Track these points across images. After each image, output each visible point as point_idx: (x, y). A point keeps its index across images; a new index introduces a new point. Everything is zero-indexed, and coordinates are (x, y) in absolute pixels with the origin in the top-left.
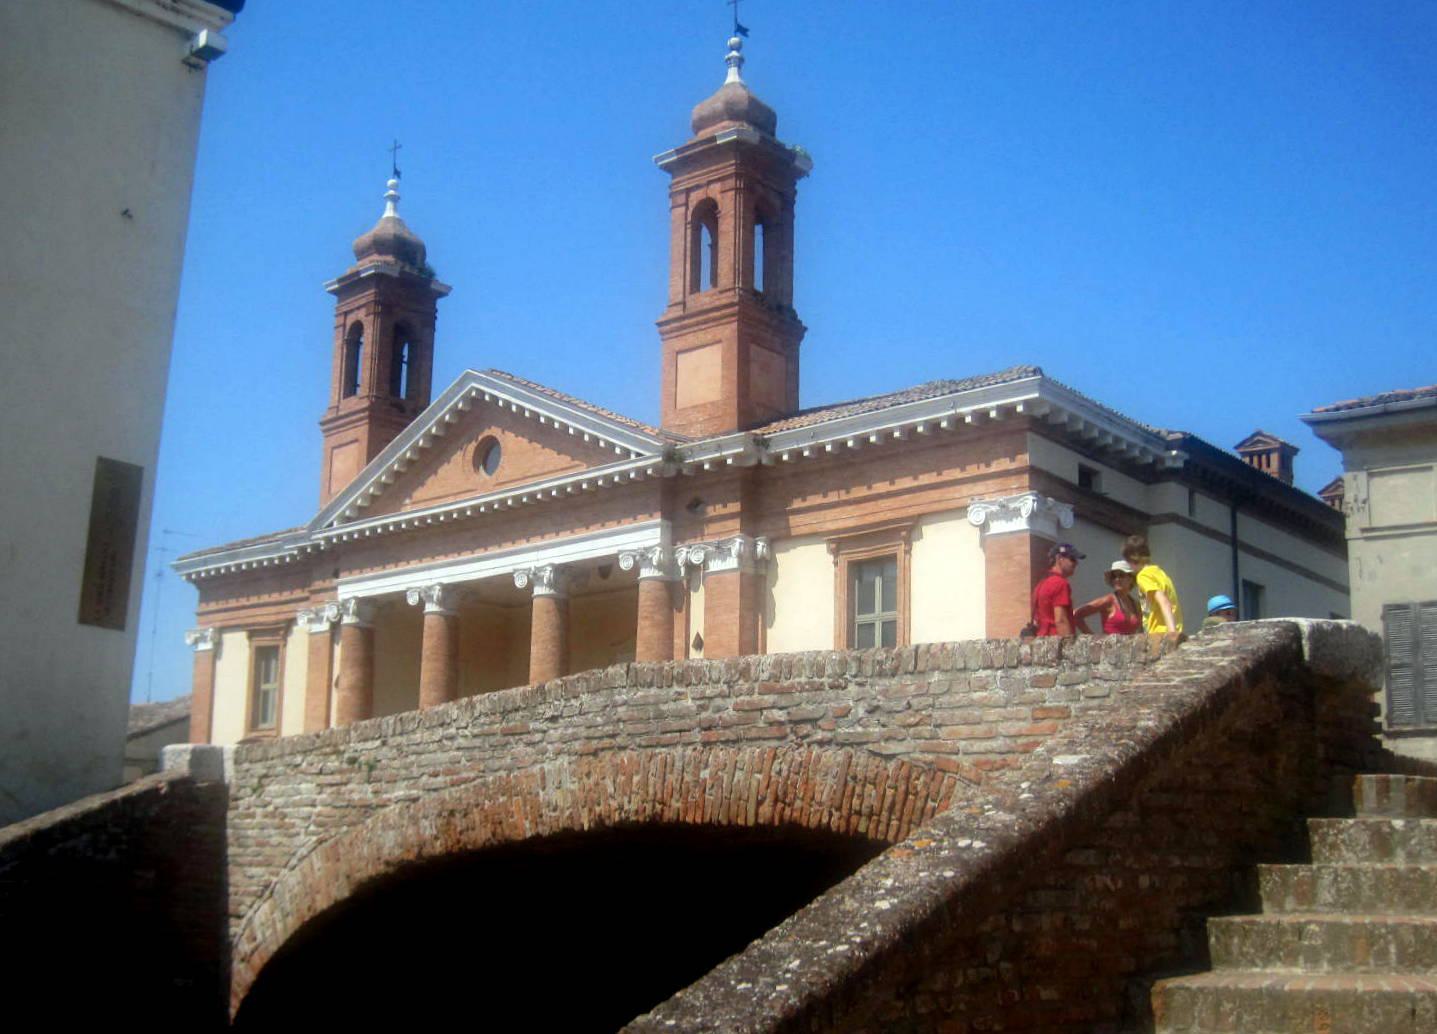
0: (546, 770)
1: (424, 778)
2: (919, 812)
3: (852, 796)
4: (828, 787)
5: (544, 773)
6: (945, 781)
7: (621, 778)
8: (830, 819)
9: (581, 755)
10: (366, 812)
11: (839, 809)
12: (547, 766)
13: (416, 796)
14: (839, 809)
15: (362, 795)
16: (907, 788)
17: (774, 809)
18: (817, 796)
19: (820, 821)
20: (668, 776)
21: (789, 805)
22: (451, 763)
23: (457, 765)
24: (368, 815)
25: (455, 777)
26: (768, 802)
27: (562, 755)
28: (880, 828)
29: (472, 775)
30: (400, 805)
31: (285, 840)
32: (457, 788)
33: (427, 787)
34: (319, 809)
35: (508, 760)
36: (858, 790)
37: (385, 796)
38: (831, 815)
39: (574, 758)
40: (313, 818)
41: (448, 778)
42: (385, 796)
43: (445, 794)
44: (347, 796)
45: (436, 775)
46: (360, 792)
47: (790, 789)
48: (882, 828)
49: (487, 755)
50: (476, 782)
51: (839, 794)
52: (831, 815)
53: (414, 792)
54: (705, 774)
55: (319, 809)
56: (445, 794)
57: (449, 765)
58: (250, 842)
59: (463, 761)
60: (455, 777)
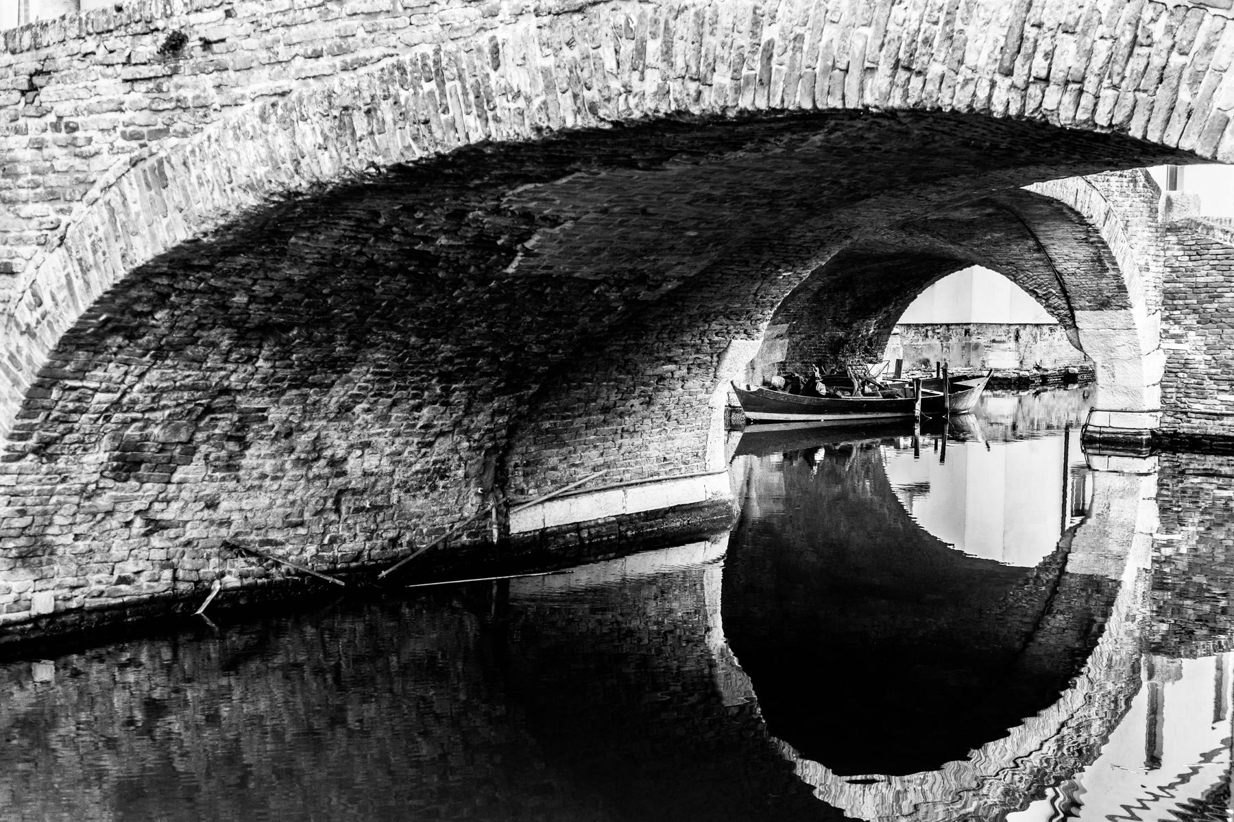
0: (500, 42)
1: (299, 61)
2: (1155, 75)
3: (1031, 57)
4: (990, 42)
5: (496, 46)
6: (1206, 24)
7: (628, 47)
8: (990, 97)
9: (558, 14)
10: (205, 116)
11: (1009, 73)
12: (501, 34)
13: (286, 89)
14: (1009, 73)
15: (197, 92)
16: (1136, 37)
17: (892, 84)
18: (970, 60)
19: (974, 95)
20: (707, 38)
21: (919, 73)
22: (341, 37)
23: (350, 40)
24: (208, 120)
25: (349, 58)
26: (884, 69)
27: (526, 16)
28: (1083, 102)
29: (377, 52)
30: (259, 103)
31: (77, 162)
32: (352, 74)
33: (303, 75)
34: (127, 116)
35: (436, 28)
36: (1045, 46)
37: (237, 91)
38: (993, 84)
39: (546, 20)
40: (121, 128)
41: (338, 61)
42: (237, 91)
43: (334, 83)
44: (173, 94)
45: (317, 55)
46: (196, 87)
47: (921, 49)
48: (1086, 101)
49: (402, 21)
50: (382, 64)
51: (1010, 51)
52: (993, 84)
53: (284, 84)
54: (769, 33)
55: (127, 116)
56: (334, 83)
57: (338, 40)
58: (20, 169)
59: (361, 33)
60: (349, 58)
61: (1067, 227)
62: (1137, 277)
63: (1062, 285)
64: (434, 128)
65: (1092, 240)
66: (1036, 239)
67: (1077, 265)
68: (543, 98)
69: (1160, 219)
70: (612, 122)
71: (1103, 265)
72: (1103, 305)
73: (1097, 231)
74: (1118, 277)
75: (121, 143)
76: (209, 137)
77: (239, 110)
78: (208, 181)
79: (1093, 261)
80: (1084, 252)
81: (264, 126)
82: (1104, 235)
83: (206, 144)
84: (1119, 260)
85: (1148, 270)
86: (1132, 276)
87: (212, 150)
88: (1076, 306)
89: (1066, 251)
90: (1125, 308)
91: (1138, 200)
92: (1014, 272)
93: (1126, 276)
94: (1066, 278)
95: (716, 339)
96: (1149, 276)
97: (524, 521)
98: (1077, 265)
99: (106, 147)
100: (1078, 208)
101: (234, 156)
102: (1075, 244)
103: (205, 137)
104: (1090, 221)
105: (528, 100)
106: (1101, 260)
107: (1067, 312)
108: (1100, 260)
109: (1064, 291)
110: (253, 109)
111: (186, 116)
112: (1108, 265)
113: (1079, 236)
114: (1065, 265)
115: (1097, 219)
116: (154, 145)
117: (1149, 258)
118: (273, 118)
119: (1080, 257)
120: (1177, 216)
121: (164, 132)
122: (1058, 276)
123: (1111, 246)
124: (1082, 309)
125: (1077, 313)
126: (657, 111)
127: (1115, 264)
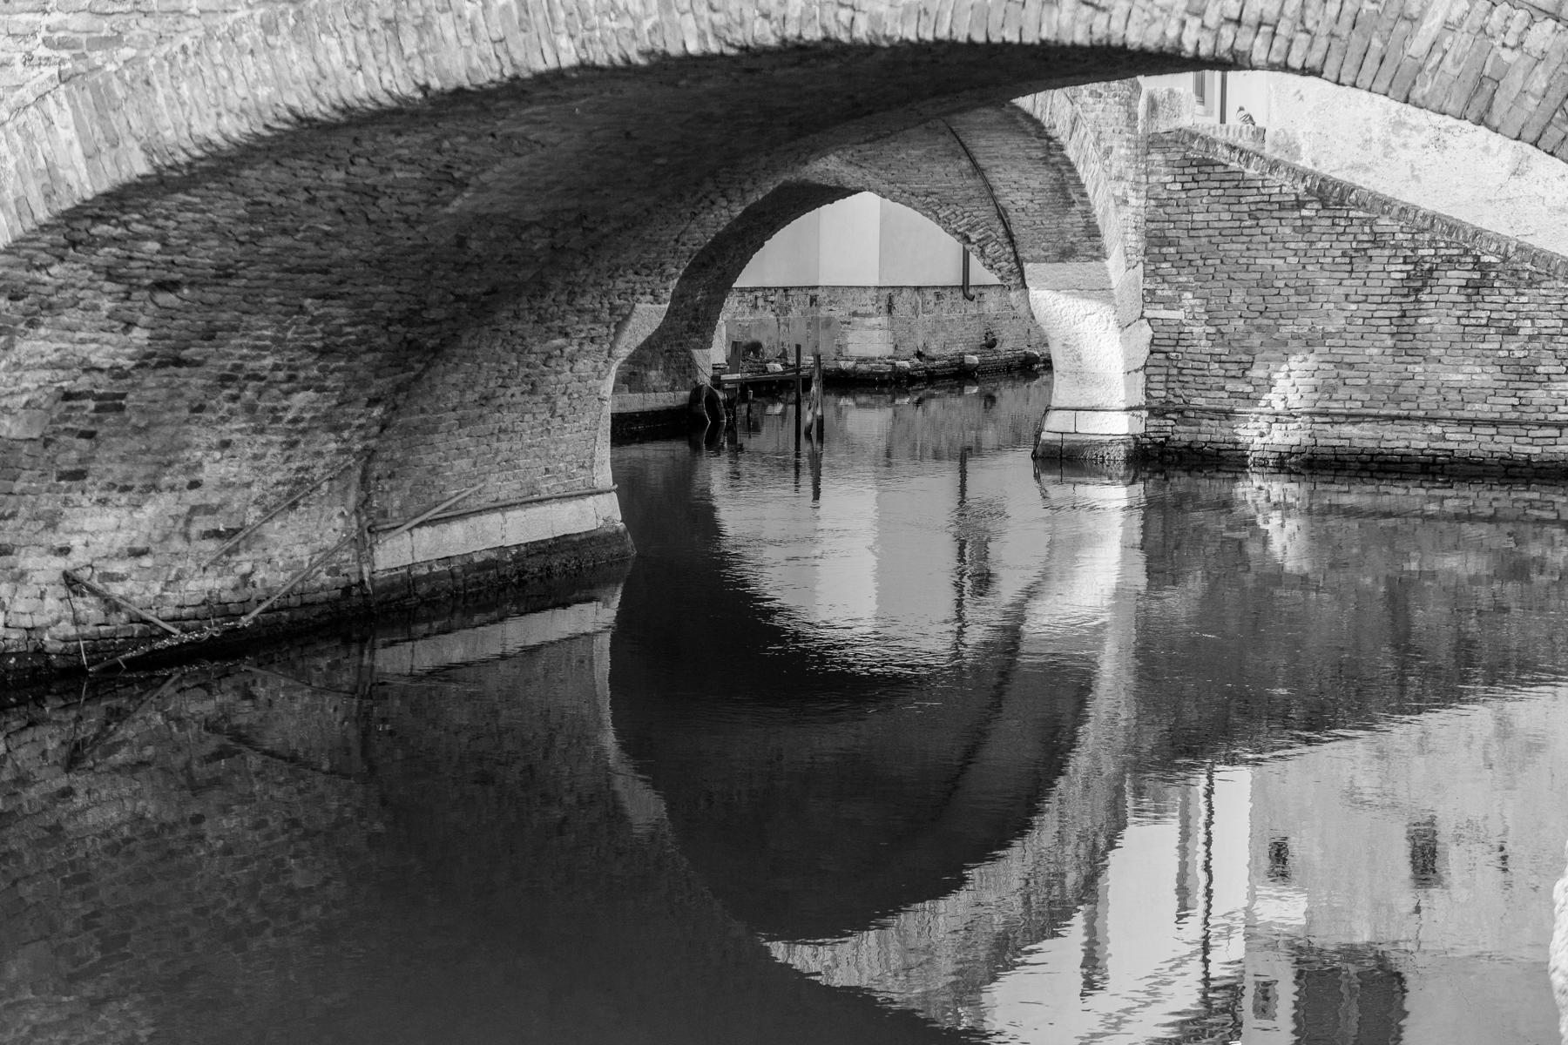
61: (1018, 140)
62: (1112, 213)
63: (1006, 225)
64: (512, 47)
65: (1052, 160)
66: (972, 160)
67: (1029, 196)
68: (656, 18)
69: (1139, 128)
70: (741, 48)
71: (1067, 197)
72: (1066, 254)
73: (1061, 148)
74: (1087, 214)
75: (42, 52)
76: (184, 49)
77: (230, 19)
78: (183, 104)
79: (1053, 190)
80: (1040, 179)
81: (271, 39)
82: (1071, 153)
83: (180, 57)
84: (1089, 190)
85: (1126, 202)
86: (1106, 211)
87: (191, 65)
88: (1026, 255)
89: (1015, 175)
90: (1096, 258)
91: (1111, 101)
92: (931, 204)
93: (1098, 211)
94: (1012, 214)
95: (618, 302)
96: (1128, 212)
97: (405, 551)
98: (1029, 196)
99: (19, 57)
100: (1037, 115)
101: (224, 74)
102: (1027, 165)
103: (176, 48)
104: (1053, 133)
105: (637, 20)
106: (1065, 187)
107: (1014, 265)
108: (1063, 188)
109: (1009, 234)
110: (251, 16)
111: (147, 23)
112: (1075, 197)
113: (1034, 154)
114: (1012, 197)
115: (1060, 131)
116: (97, 57)
117: (1128, 185)
118: (284, 30)
119: (1035, 184)
120: (1162, 126)
121: (116, 40)
122: (1002, 215)
123: (1080, 169)
124: (1036, 260)
125: (1027, 267)
126: (800, 37)
127: (1084, 195)
